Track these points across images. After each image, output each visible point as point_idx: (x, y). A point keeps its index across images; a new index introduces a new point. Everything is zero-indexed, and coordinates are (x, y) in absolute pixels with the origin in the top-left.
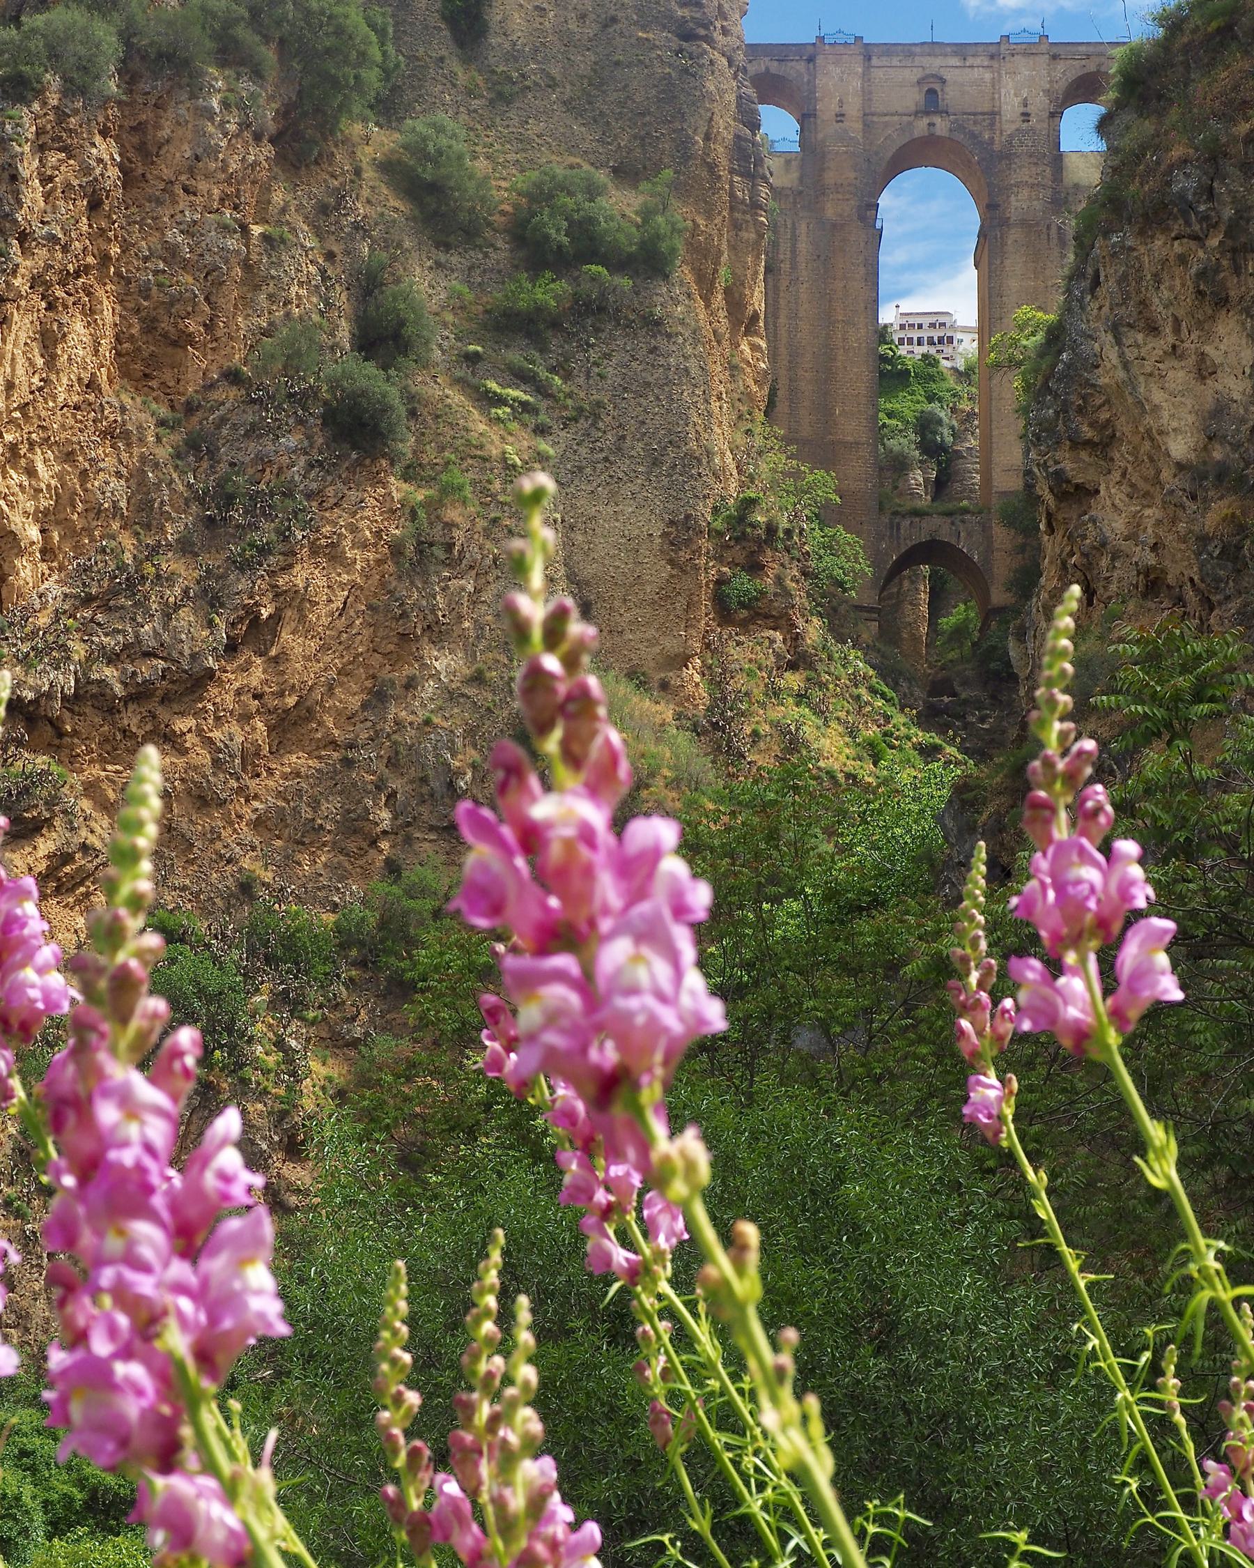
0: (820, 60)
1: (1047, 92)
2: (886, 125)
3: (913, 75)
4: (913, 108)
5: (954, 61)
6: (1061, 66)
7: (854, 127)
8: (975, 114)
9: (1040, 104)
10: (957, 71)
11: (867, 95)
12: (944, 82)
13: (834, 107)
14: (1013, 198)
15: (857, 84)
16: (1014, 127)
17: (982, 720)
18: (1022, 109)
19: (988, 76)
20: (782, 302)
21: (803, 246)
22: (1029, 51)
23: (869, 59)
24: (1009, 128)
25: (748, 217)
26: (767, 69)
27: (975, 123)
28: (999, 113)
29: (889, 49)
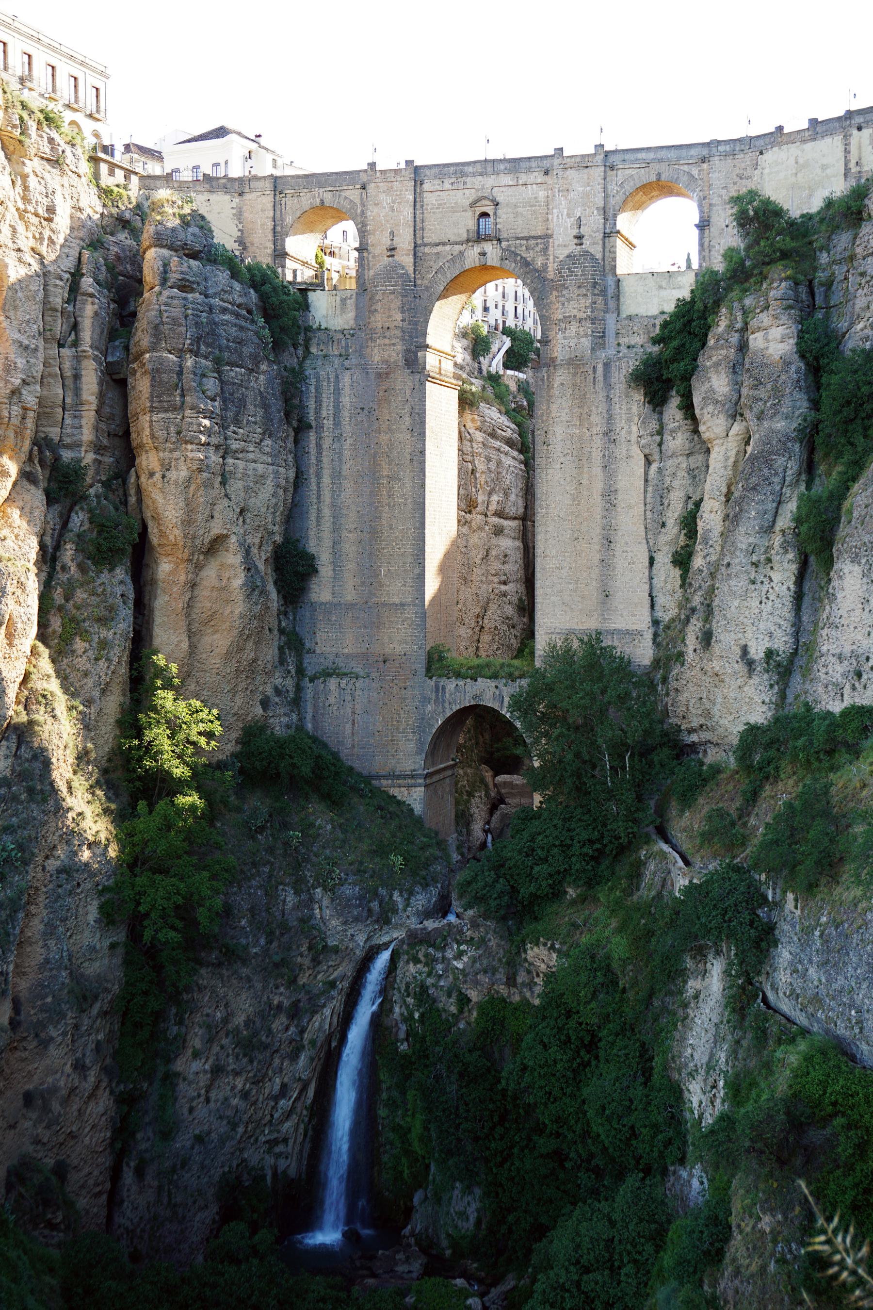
0: (371, 187)
4: (465, 236)
5: (507, 180)
7: (407, 261)
8: (527, 239)
9: (593, 224)
11: (417, 228)
15: (407, 212)
16: (566, 252)
18: (575, 232)
20: (325, 460)
21: (346, 400)
22: (583, 163)
24: (562, 254)
25: (177, 454)
29: (443, 171)
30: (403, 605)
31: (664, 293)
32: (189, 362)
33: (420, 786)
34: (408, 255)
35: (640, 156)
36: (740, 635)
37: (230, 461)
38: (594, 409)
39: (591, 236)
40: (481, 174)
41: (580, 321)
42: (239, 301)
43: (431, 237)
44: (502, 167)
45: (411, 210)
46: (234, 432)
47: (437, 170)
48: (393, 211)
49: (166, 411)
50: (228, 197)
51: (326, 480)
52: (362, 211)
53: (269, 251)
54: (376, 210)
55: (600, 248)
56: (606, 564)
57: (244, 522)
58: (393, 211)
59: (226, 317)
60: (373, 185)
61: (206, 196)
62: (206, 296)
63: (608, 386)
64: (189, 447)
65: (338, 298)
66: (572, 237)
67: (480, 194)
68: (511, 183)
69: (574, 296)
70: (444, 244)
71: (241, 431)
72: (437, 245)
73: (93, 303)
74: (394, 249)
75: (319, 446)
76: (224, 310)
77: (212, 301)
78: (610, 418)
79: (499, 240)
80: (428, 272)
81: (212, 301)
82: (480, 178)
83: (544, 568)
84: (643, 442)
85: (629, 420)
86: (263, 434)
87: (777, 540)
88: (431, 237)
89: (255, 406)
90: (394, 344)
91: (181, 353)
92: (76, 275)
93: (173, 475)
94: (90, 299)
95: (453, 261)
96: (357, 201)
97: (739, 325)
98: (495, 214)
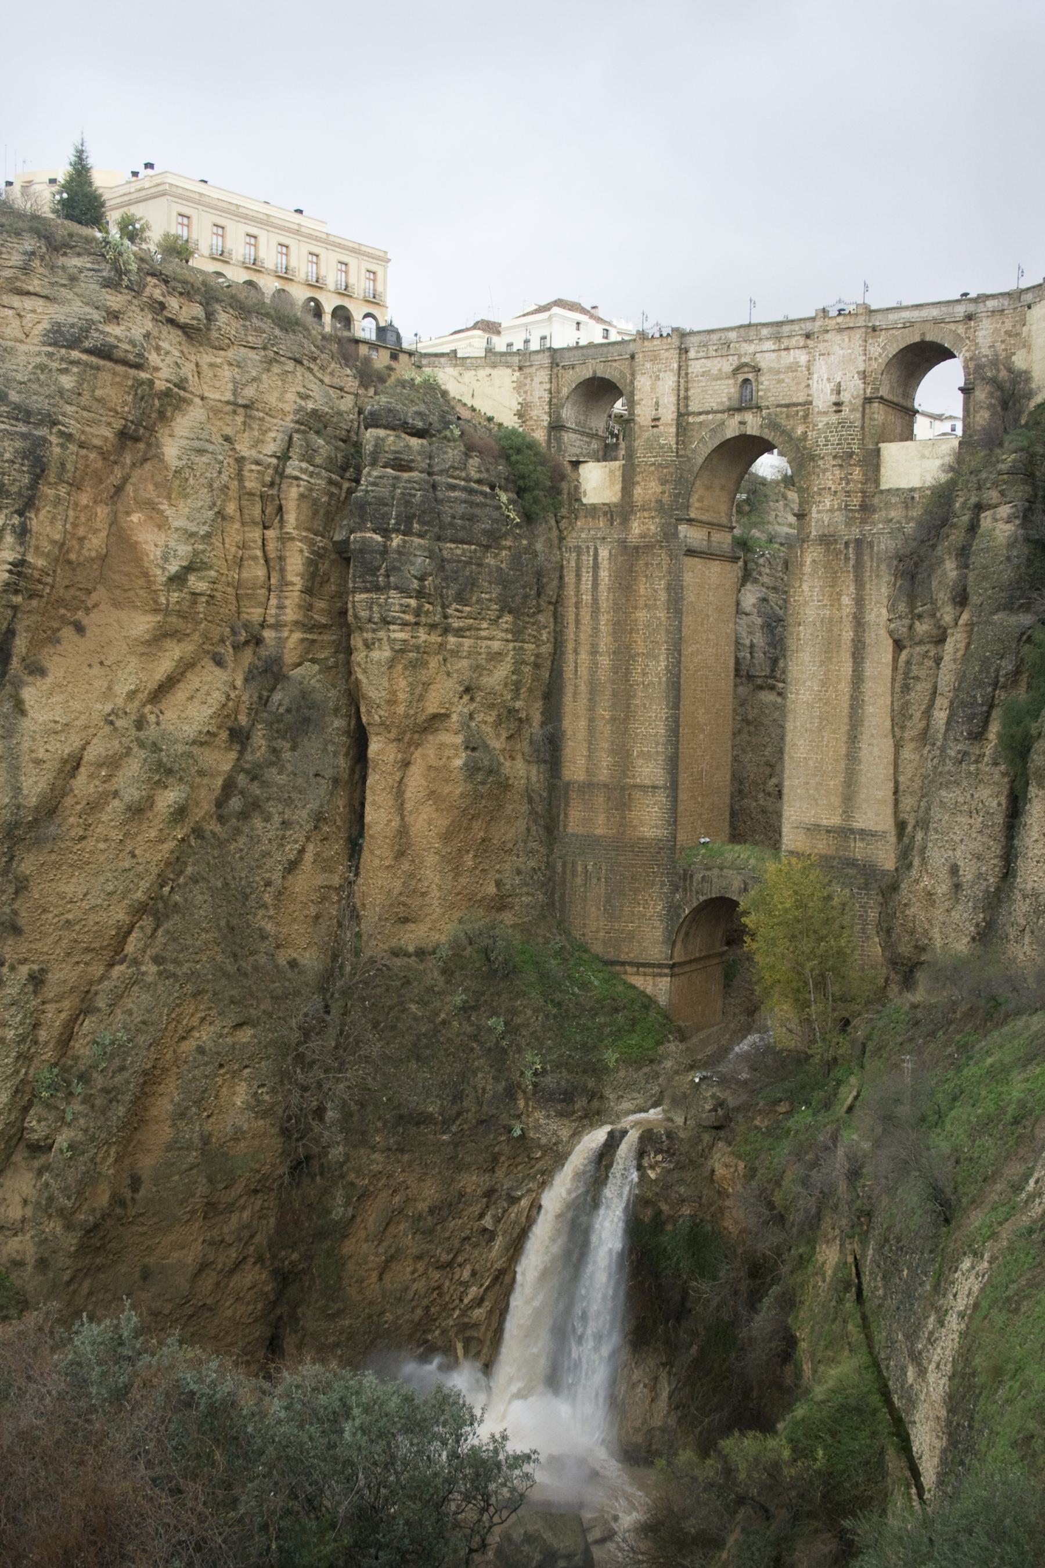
0: (639, 357)
1: (864, 375)
3: (727, 365)
5: (769, 345)
6: (883, 337)
8: (787, 406)
9: (854, 389)
10: (773, 355)
12: (757, 370)
14: (814, 509)
16: (825, 419)
17: (652, 1167)
18: (834, 398)
19: (803, 358)
21: (604, 574)
24: (821, 422)
25: (382, 634)
26: (595, 372)
27: (787, 417)
28: (811, 403)
30: (654, 787)
32: (396, 541)
33: (666, 975)
36: (950, 853)
37: (452, 639)
42: (477, 476)
43: (693, 407)
44: (765, 332)
45: (675, 378)
46: (457, 610)
49: (367, 590)
50: (509, 371)
51: (584, 656)
53: (546, 424)
55: (859, 415)
56: (852, 757)
57: (472, 699)
59: (456, 494)
61: (488, 371)
62: (430, 474)
64: (392, 627)
67: (744, 360)
70: (707, 413)
71: (468, 609)
72: (700, 413)
73: (298, 486)
74: (658, 419)
75: (577, 622)
76: (453, 488)
77: (437, 478)
78: (859, 602)
79: (759, 408)
80: (691, 443)
81: (437, 478)
83: (791, 757)
86: (502, 610)
87: (990, 747)
88: (693, 407)
89: (490, 583)
90: (653, 518)
91: (385, 533)
92: (284, 457)
93: (375, 655)
94: (295, 482)
96: (627, 372)
97: (973, 500)
98: (757, 380)
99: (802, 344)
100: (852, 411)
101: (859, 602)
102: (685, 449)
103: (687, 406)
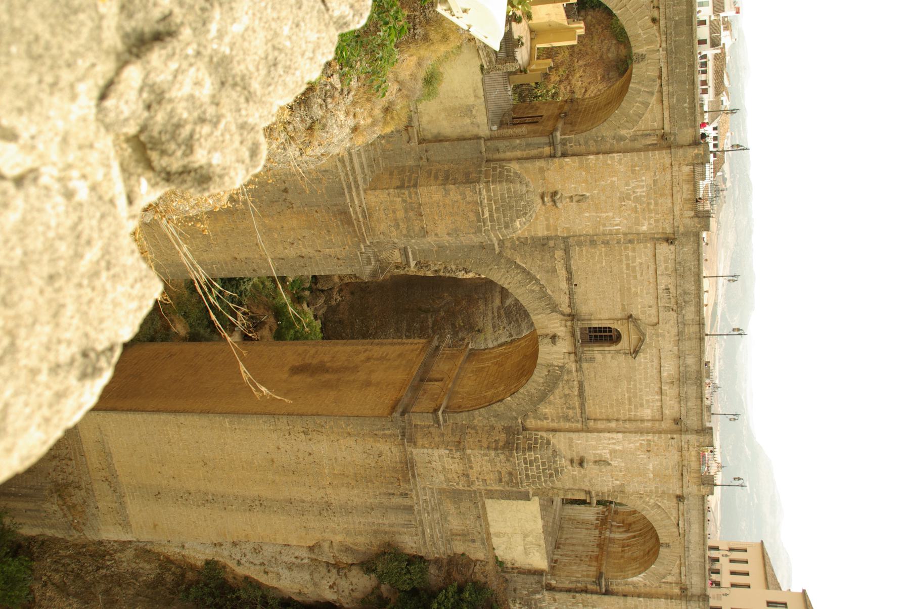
2: (555, 271)
4: (584, 309)
5: (669, 368)
8: (581, 394)
13: (569, 188)
14: (443, 452)
15: (618, 223)
18: (590, 456)
19: (647, 413)
23: (670, 240)
24: (559, 441)
26: (642, 57)
31: (519, 539)
34: (548, 229)
35: (695, 528)
38: (356, 491)
39: (585, 476)
40: (680, 334)
41: (468, 476)
43: (581, 259)
44: (691, 361)
47: (691, 264)
48: (622, 199)
52: (622, 138)
54: (622, 168)
56: (185, 497)
58: (622, 199)
60: (667, 161)
63: (386, 509)
65: (471, 100)
66: (582, 454)
67: (649, 331)
68: (665, 374)
69: (498, 468)
70: (569, 280)
82: (674, 331)
84: (326, 545)
85: (347, 532)
90: (397, 226)
95: (543, 295)
96: (642, 125)
99: (667, 412)
100: (574, 478)
101: (347, 510)
102: (514, 248)
103: (580, 244)
